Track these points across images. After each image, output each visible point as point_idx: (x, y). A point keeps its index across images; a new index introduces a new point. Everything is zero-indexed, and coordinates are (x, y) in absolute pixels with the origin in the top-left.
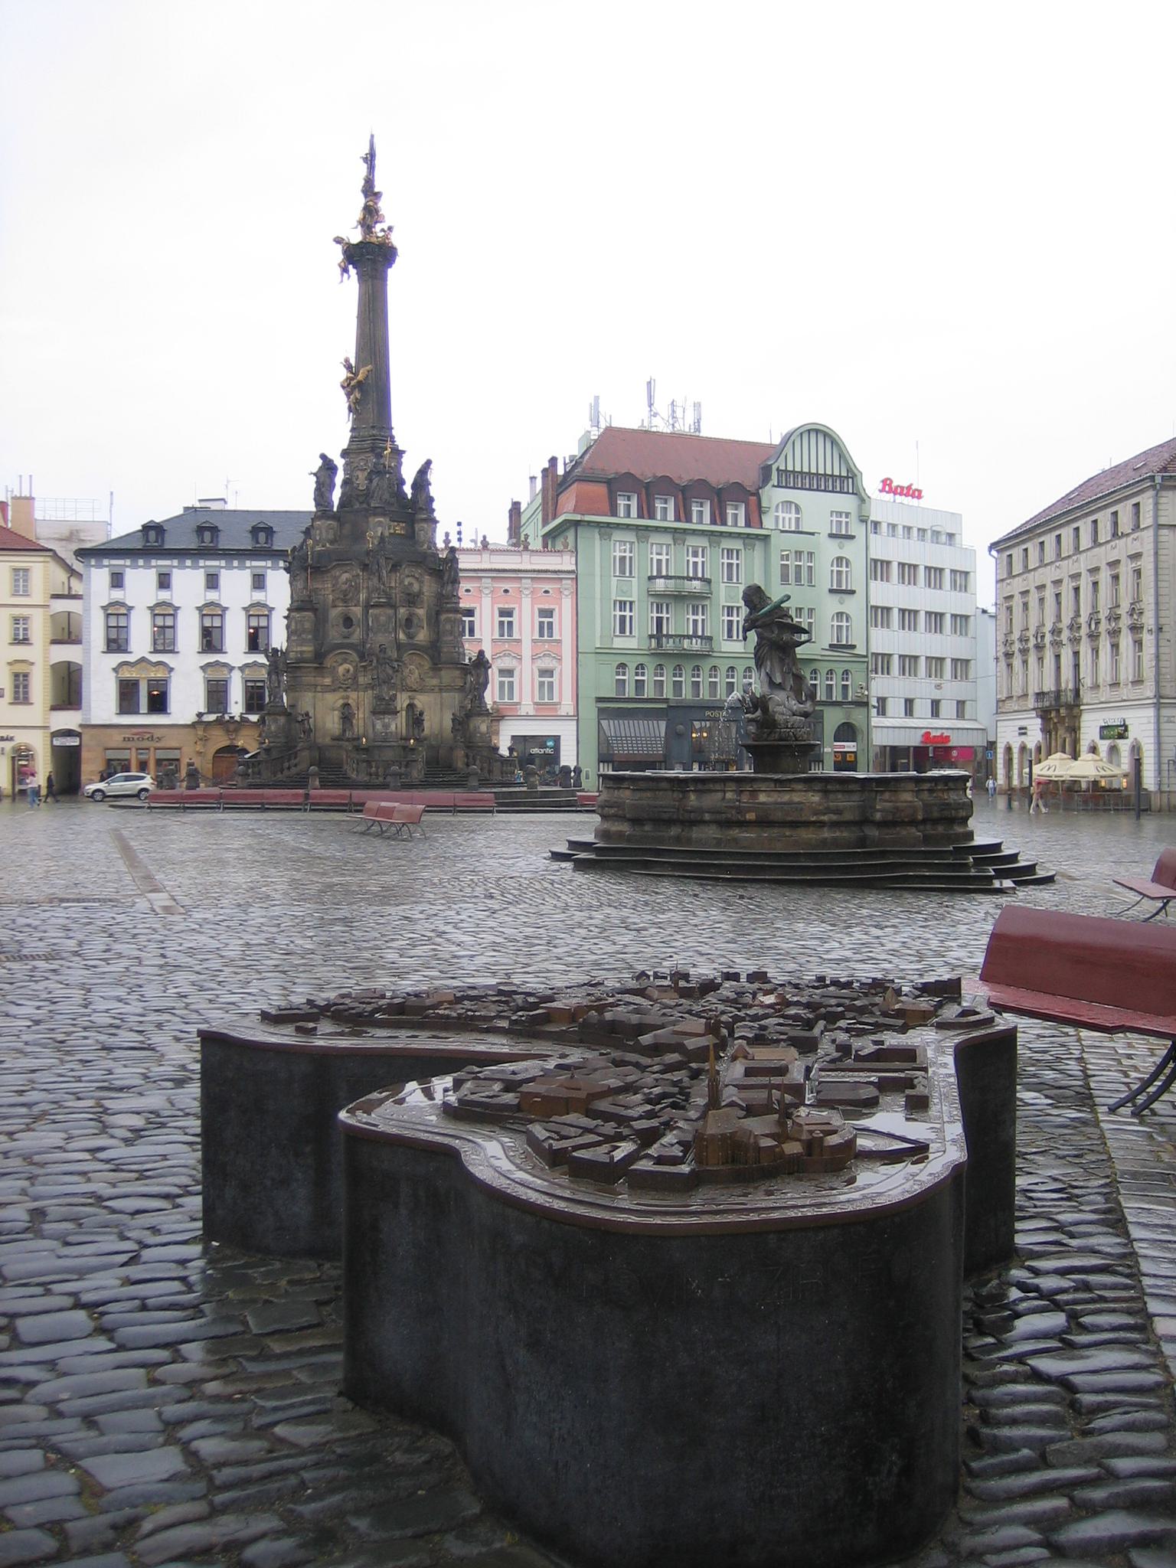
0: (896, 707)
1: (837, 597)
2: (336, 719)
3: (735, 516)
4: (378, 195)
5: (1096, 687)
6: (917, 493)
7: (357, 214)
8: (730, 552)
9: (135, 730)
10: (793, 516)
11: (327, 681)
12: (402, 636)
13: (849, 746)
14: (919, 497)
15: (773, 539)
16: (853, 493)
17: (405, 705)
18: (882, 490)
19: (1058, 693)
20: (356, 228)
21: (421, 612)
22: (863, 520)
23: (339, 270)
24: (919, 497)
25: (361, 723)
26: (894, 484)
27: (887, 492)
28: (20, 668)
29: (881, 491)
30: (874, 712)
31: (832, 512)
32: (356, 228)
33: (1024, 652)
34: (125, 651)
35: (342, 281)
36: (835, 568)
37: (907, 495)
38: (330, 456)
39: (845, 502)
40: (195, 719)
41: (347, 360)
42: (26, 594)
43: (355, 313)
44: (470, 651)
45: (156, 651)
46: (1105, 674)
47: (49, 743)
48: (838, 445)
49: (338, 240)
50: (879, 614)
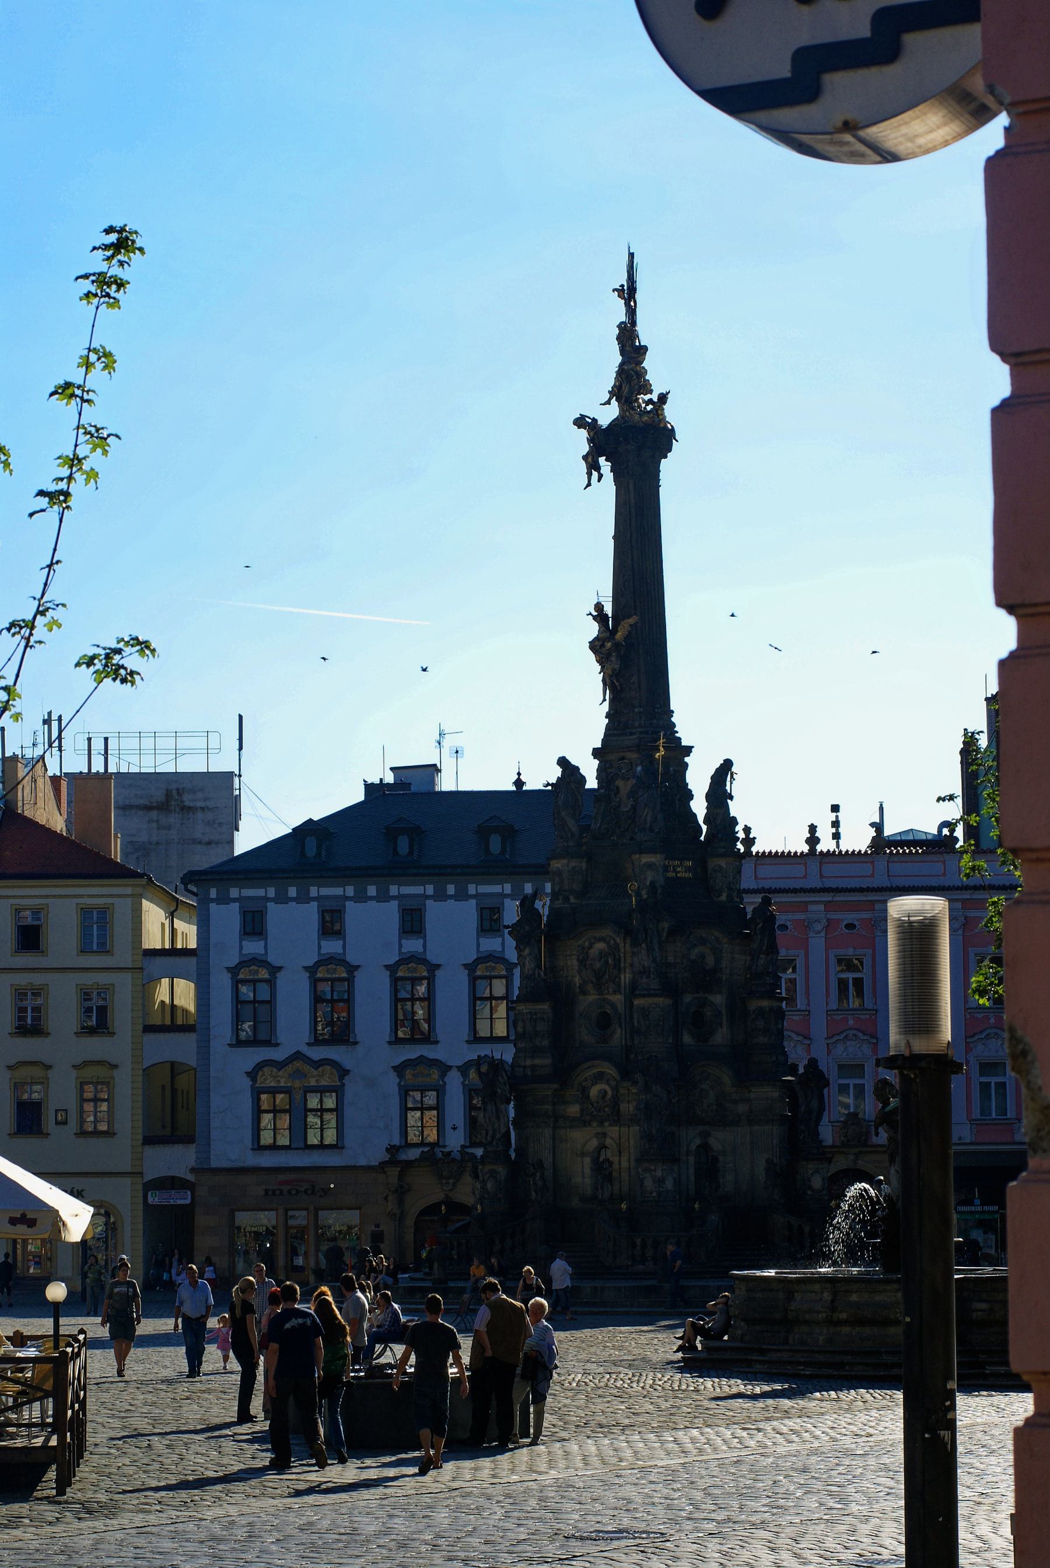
2: (587, 1170)
4: (643, 350)
7: (609, 380)
9: (282, 1177)
11: (574, 1110)
12: (687, 1039)
17: (693, 1147)
20: (608, 402)
21: (718, 999)
23: (583, 466)
25: (625, 1176)
28: (90, 1072)
32: (608, 402)
34: (269, 1043)
35: (589, 485)
38: (574, 762)
40: (387, 1157)
41: (599, 607)
42: (104, 949)
43: (610, 530)
44: (798, 1055)
45: (317, 1041)
47: (141, 1200)
49: (580, 422)
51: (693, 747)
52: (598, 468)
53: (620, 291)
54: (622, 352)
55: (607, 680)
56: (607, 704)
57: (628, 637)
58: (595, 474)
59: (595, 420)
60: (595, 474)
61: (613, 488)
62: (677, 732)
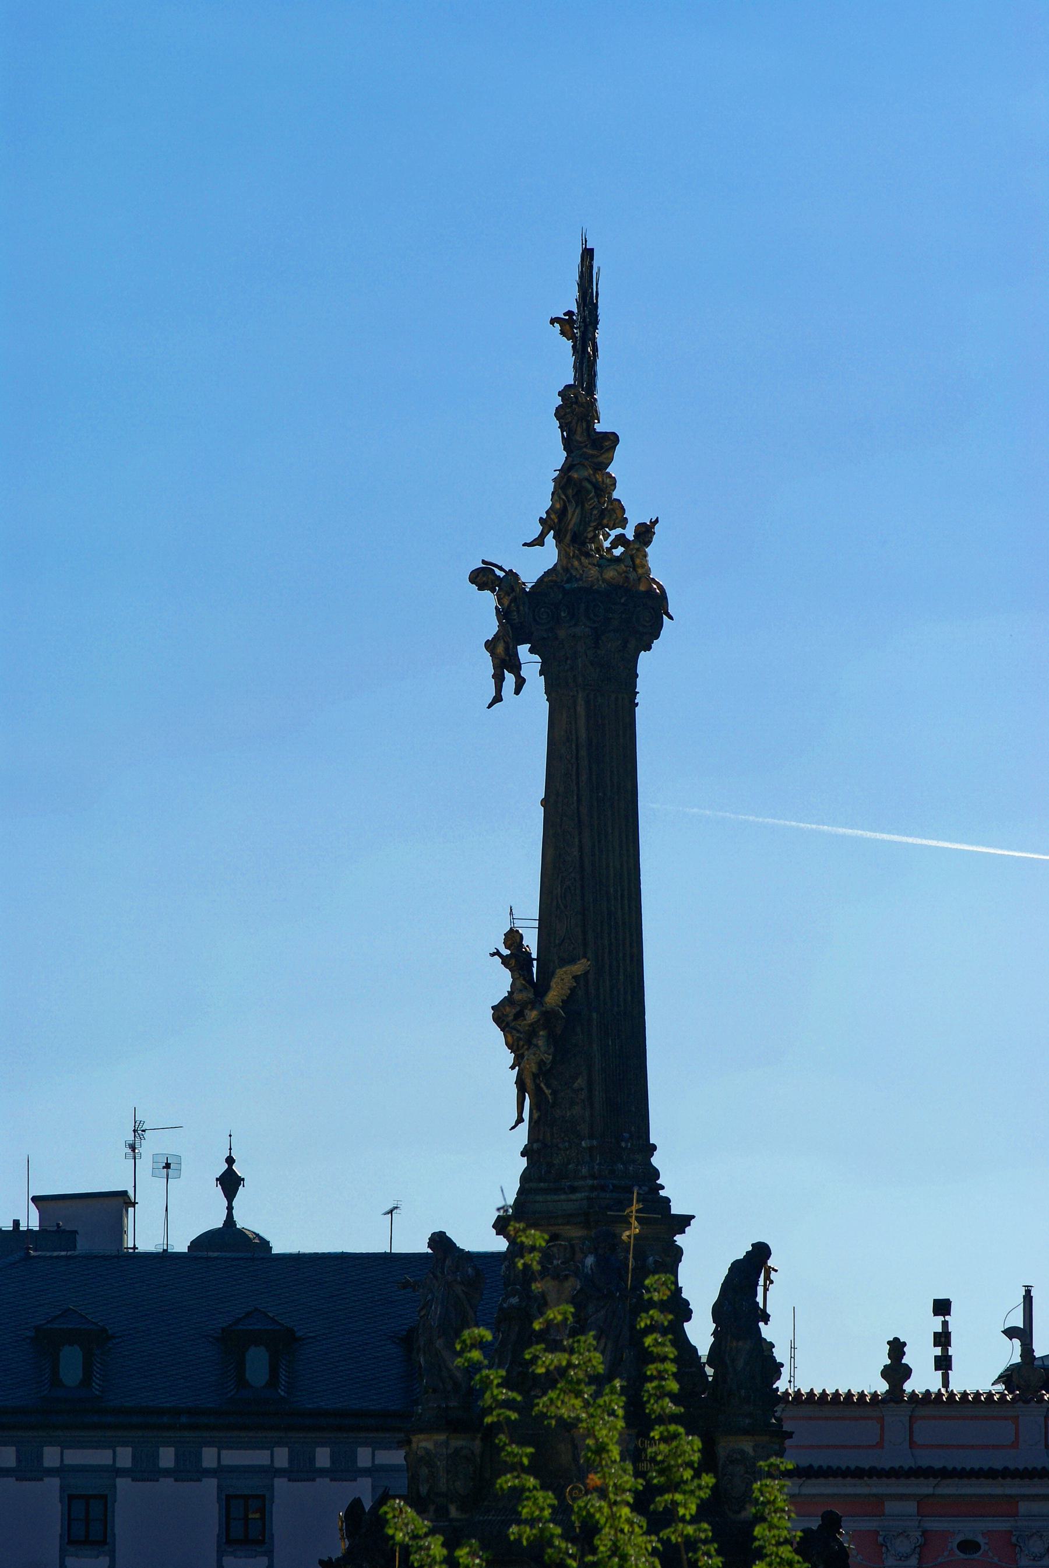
7: (543, 503)
20: (539, 541)
23: (486, 664)
32: (539, 541)
35: (498, 698)
41: (513, 938)
51: (693, 1217)
52: (515, 667)
53: (566, 324)
54: (567, 444)
55: (529, 1082)
56: (524, 1127)
57: (566, 1002)
58: (510, 678)
59: (512, 575)
60: (510, 678)
61: (543, 706)
62: (662, 1187)
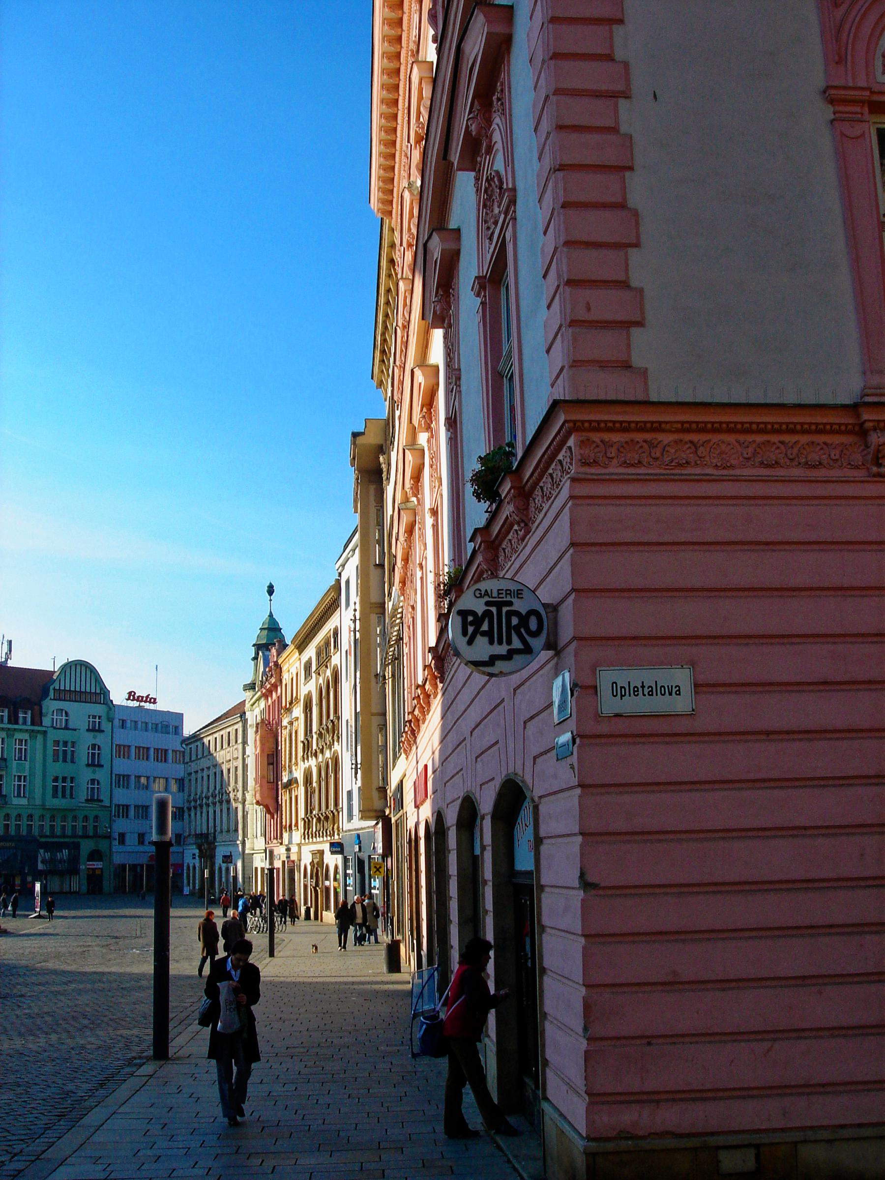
0: (132, 840)
1: (91, 769)
3: (25, 718)
5: (222, 832)
6: (152, 700)
8: (21, 741)
10: (64, 718)
13: (98, 865)
14: (155, 702)
15: (49, 735)
16: (104, 704)
18: (128, 699)
19: (208, 834)
22: (111, 720)
24: (155, 702)
26: (137, 695)
27: (132, 700)
29: (127, 700)
30: (117, 842)
31: (89, 716)
33: (195, 808)
36: (91, 751)
37: (146, 702)
39: (99, 709)
46: (225, 828)
48: (94, 673)
50: (123, 780)
